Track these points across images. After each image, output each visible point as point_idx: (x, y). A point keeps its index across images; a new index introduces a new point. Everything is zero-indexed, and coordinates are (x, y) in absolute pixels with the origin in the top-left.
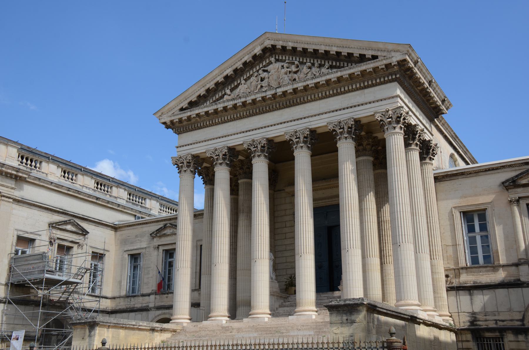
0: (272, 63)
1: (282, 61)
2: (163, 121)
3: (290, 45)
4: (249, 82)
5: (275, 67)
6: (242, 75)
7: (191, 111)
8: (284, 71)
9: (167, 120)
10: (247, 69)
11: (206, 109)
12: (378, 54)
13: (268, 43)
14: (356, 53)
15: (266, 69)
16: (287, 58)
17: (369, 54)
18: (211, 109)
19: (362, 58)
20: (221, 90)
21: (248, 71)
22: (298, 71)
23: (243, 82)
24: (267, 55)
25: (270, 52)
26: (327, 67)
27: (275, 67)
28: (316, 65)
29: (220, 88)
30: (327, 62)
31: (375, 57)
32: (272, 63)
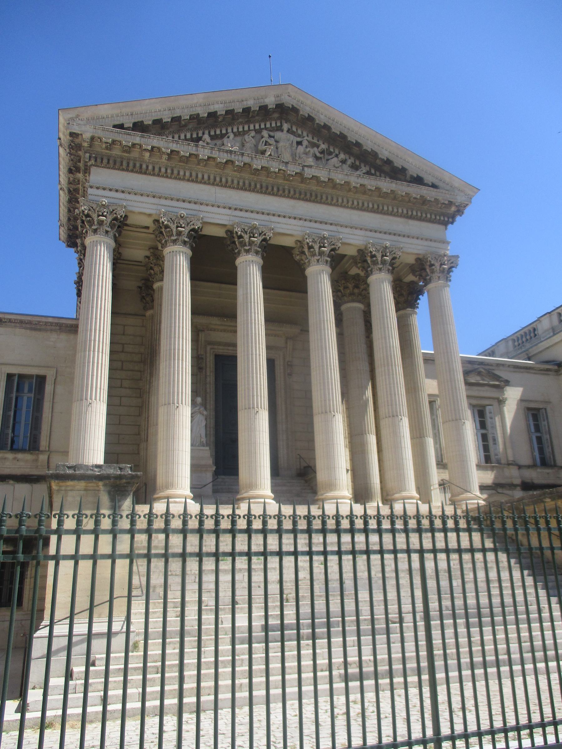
0: (282, 131)
1: (293, 133)
2: (76, 129)
3: (321, 119)
4: (239, 139)
5: (284, 138)
6: (231, 124)
7: (142, 137)
8: (301, 149)
9: (87, 132)
10: (240, 120)
11: (174, 147)
12: (440, 184)
13: (288, 101)
14: (413, 171)
15: (272, 134)
16: (305, 134)
17: (428, 179)
18: (185, 149)
19: (418, 180)
20: (191, 131)
21: (241, 123)
22: (321, 158)
23: (232, 136)
24: (276, 115)
25: (284, 114)
26: (364, 171)
27: (284, 138)
28: (349, 162)
29: (190, 126)
30: (362, 165)
31: (434, 186)
32: (282, 131)
